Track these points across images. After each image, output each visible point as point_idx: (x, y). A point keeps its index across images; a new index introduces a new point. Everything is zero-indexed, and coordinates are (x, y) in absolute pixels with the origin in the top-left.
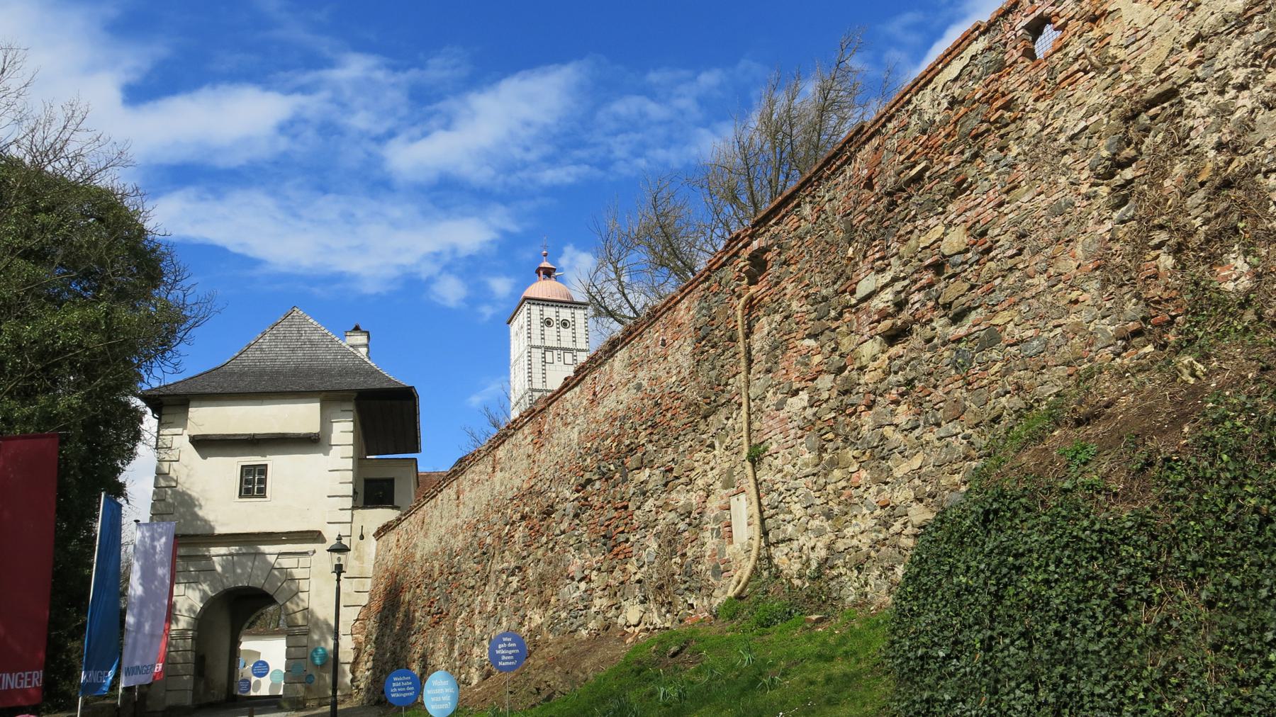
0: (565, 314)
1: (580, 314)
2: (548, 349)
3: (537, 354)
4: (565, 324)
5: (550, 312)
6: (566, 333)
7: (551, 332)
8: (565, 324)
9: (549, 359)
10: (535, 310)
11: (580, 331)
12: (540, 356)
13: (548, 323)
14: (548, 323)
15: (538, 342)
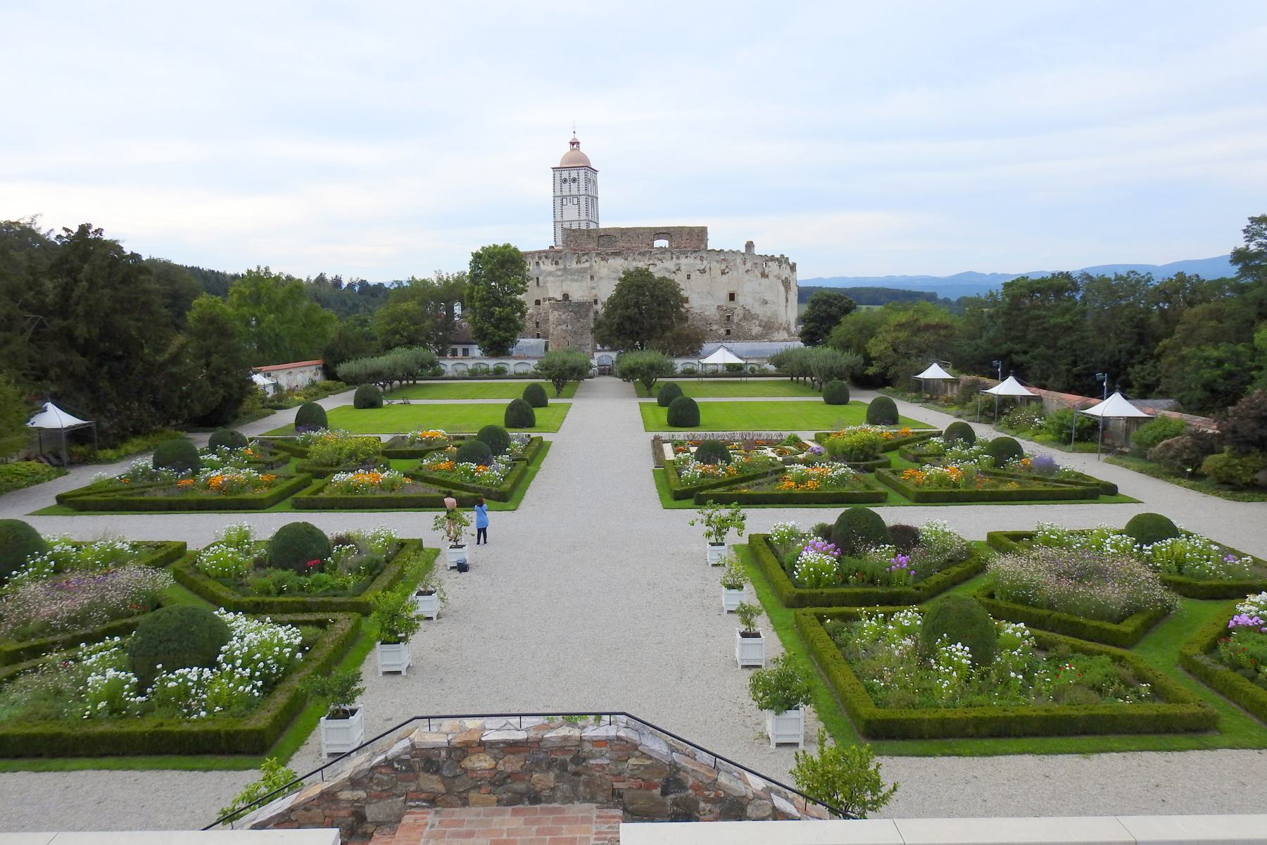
0: (574, 174)
1: (582, 172)
2: (563, 197)
3: (558, 201)
4: (574, 180)
5: (565, 174)
6: (574, 186)
7: (566, 186)
8: (574, 180)
9: (565, 203)
10: (557, 174)
11: (582, 183)
12: (560, 201)
13: (565, 181)
14: (565, 181)
15: (558, 193)
